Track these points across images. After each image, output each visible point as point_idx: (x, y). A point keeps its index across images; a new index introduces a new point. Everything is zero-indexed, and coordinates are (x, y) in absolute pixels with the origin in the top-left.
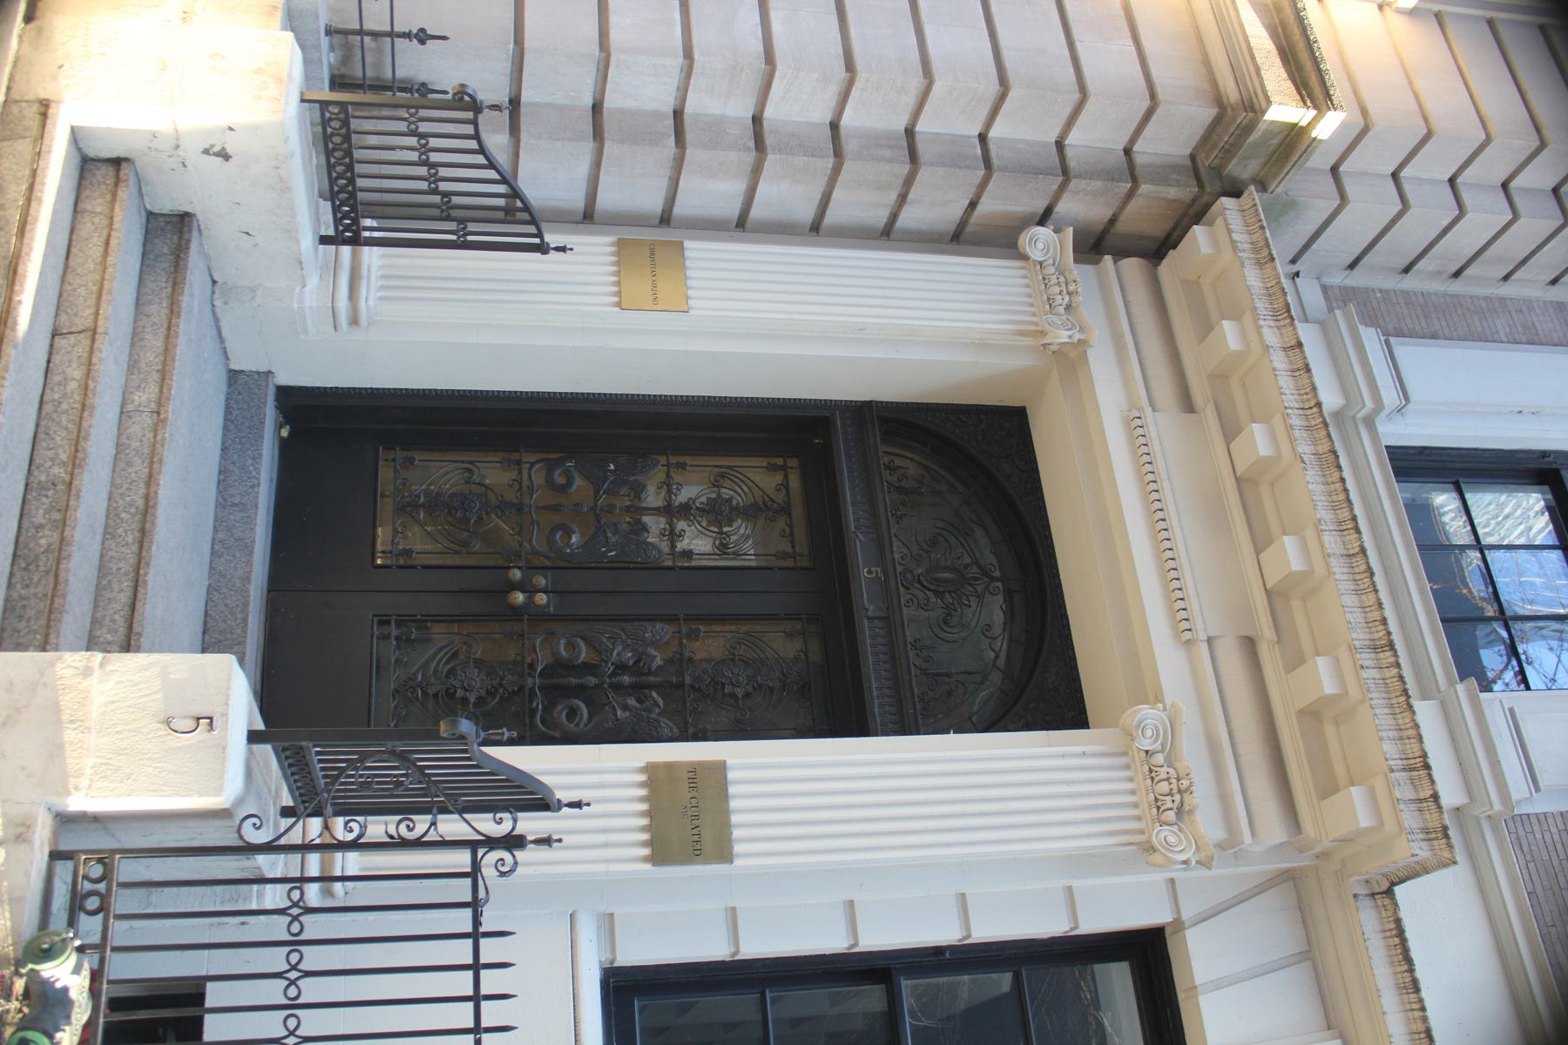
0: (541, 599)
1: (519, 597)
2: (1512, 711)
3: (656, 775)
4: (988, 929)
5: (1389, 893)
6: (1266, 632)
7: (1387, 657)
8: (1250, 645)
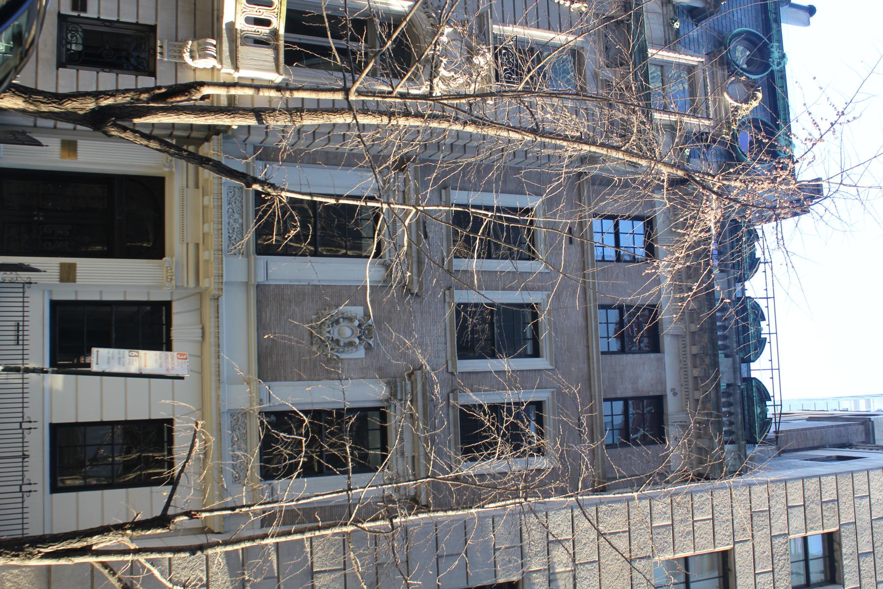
0: (41, 218)
1: (36, 218)
2: (267, 262)
3: (62, 265)
4: (130, 298)
5: (218, 299)
6: (201, 243)
7: (220, 253)
8: (197, 245)
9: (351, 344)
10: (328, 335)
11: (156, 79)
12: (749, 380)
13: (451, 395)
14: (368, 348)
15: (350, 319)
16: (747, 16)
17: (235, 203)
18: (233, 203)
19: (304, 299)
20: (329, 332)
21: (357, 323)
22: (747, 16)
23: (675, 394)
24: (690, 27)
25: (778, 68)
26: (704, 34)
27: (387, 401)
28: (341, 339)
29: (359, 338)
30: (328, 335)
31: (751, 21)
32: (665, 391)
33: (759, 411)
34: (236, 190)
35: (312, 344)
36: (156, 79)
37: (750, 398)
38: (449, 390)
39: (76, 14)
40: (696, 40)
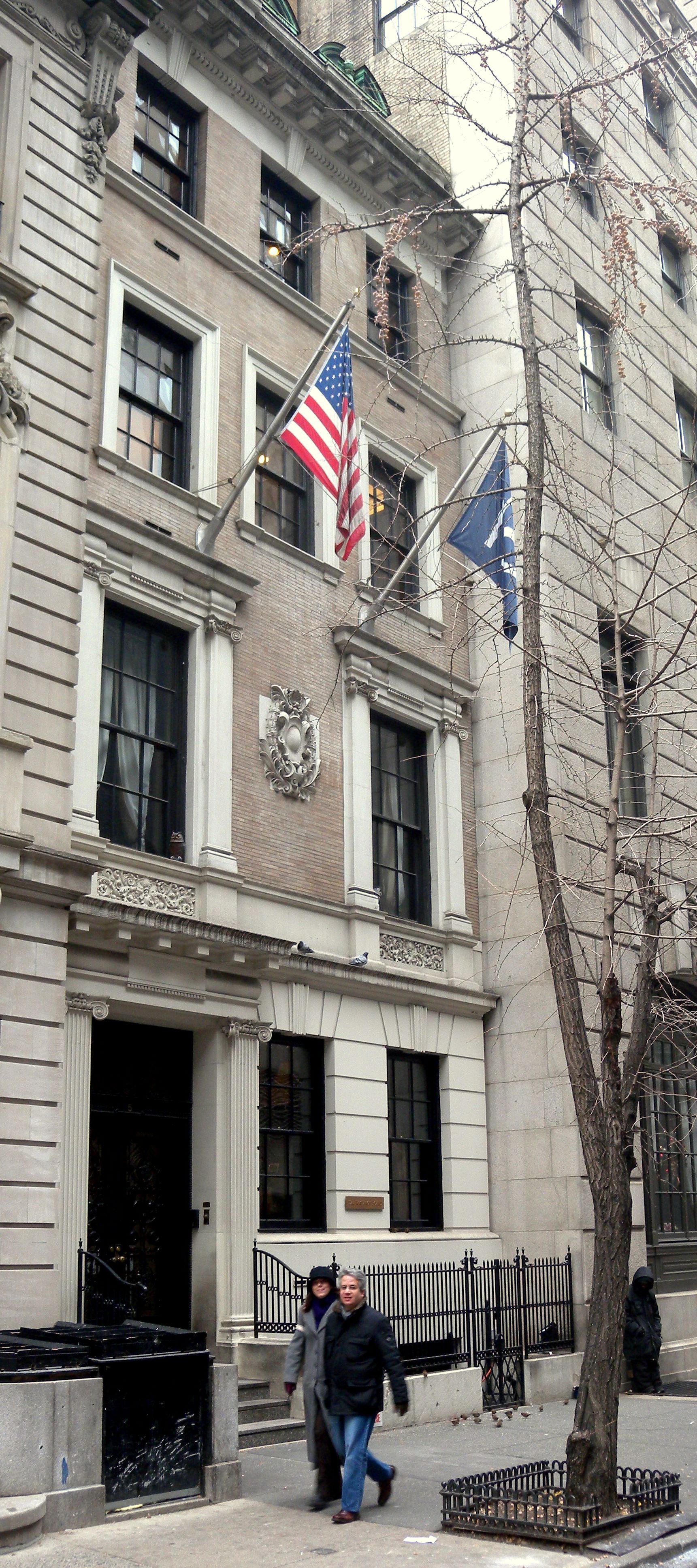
15: (281, 724)
18: (122, 889)
19: (250, 796)
35: (303, 801)
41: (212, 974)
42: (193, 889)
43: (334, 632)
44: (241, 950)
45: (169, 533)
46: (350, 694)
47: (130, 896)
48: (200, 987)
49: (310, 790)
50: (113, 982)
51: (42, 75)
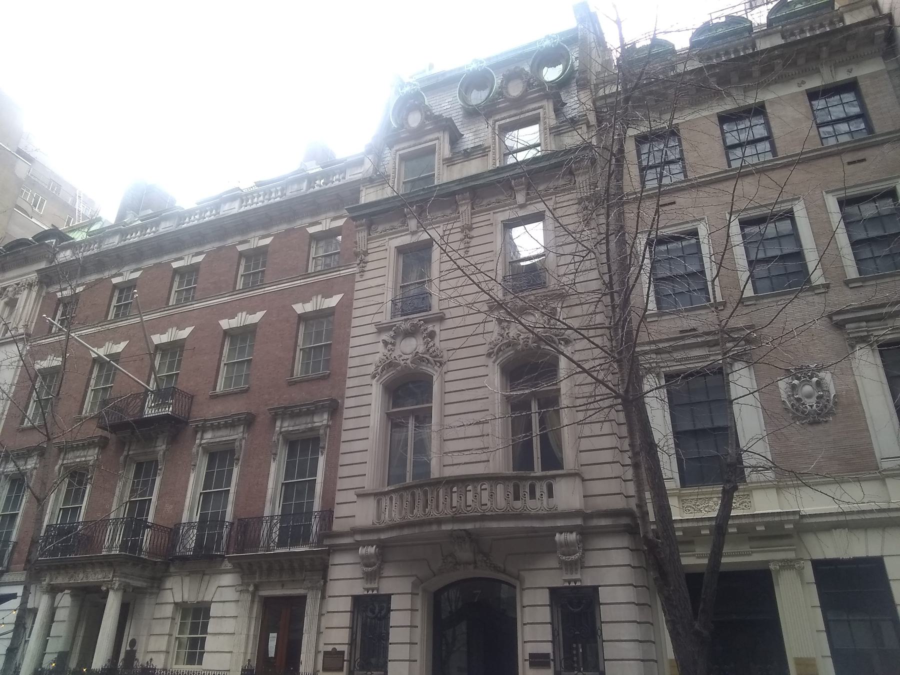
9: (819, 384)
10: (814, 407)
11: (600, 586)
12: (770, 22)
13: (851, 286)
14: (820, 369)
15: (794, 387)
16: (445, 98)
17: (698, 505)
18: (699, 507)
20: (811, 406)
21: (796, 382)
22: (445, 98)
23: (803, 83)
24: (463, 140)
25: (485, 62)
26: (469, 128)
27: (871, 345)
28: (816, 394)
29: (811, 378)
30: (814, 407)
31: (449, 94)
32: (802, 92)
33: (800, 6)
34: (685, 505)
35: (826, 422)
36: (600, 586)
37: (788, 17)
38: (845, 288)
39: (552, 663)
40: (475, 133)
41: (752, 539)
42: (748, 495)
43: (830, 317)
44: (759, 524)
45: (694, 330)
46: (853, 347)
47: (706, 509)
48: (746, 548)
49: (830, 413)
50: (690, 556)
51: (558, 206)
